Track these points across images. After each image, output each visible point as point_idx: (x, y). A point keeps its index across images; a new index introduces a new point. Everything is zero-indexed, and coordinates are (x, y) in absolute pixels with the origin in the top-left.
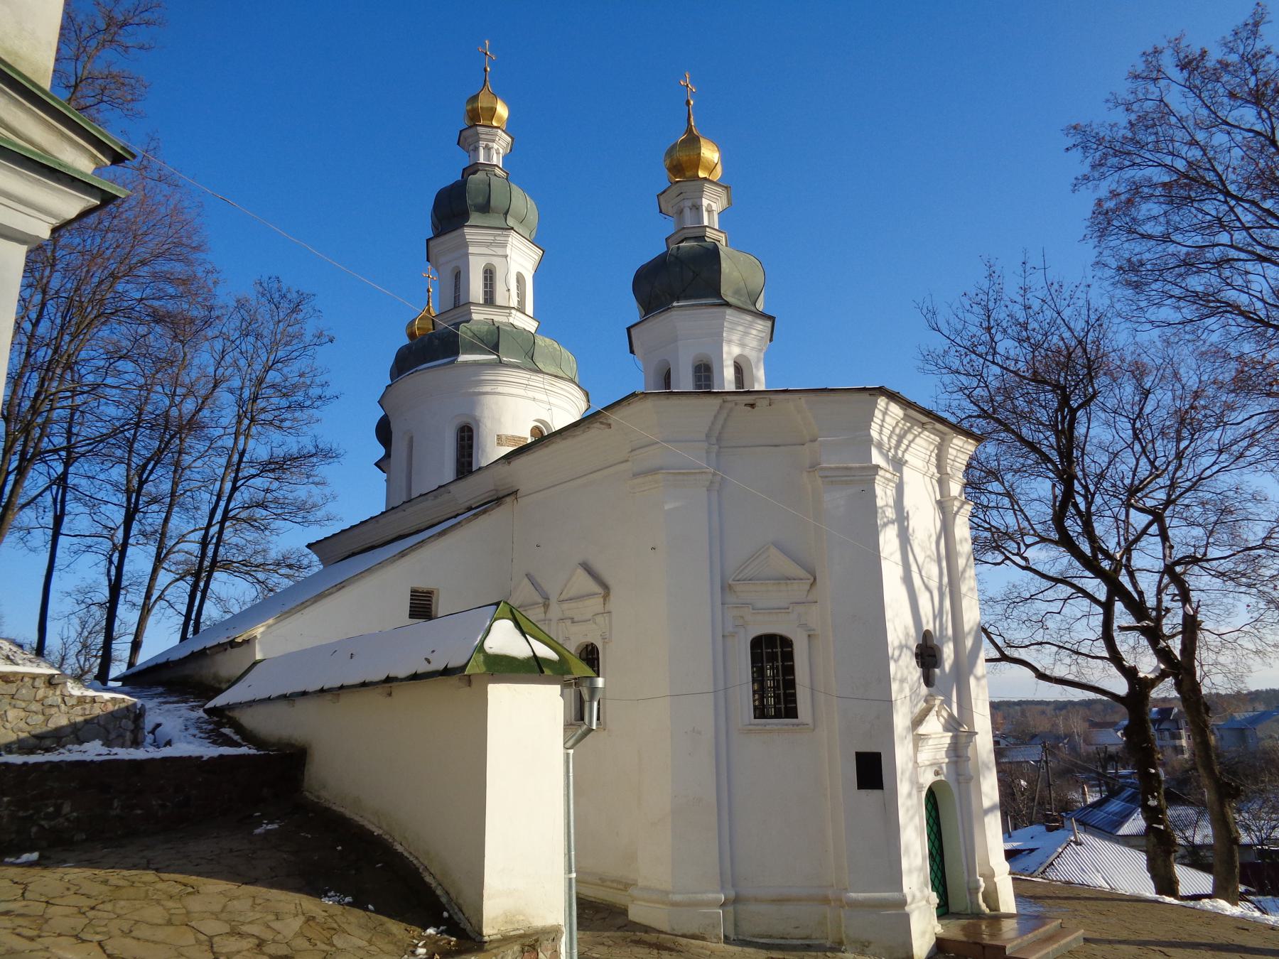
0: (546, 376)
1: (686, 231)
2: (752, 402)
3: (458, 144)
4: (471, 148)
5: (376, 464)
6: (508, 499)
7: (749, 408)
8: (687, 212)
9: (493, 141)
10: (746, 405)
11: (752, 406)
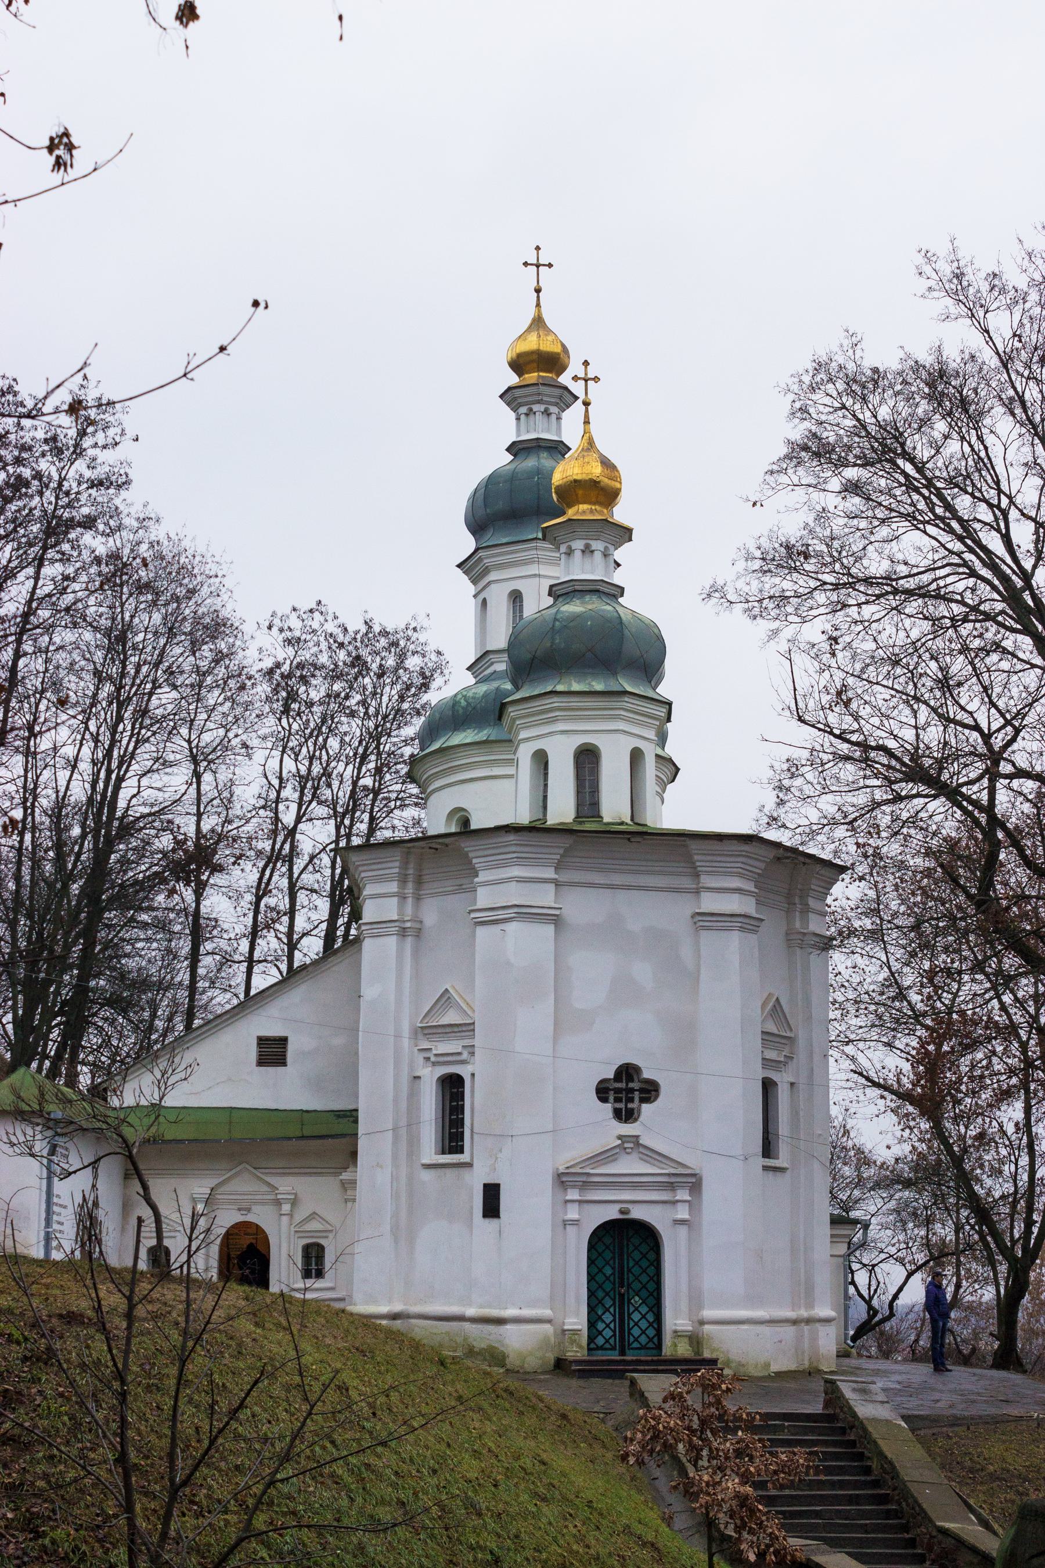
9: (539, 402)
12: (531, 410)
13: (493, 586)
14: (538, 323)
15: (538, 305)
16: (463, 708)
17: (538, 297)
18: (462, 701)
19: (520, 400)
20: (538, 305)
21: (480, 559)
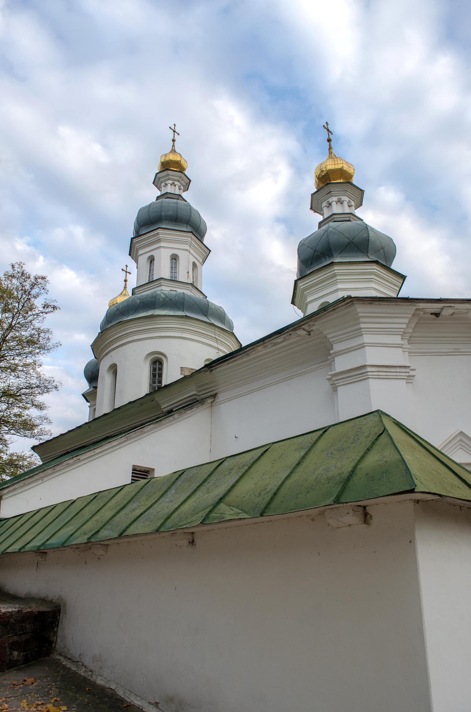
0: (217, 329)
1: (335, 216)
2: (437, 311)
3: (153, 183)
4: (163, 184)
5: (83, 395)
6: (209, 401)
7: (433, 316)
8: (334, 204)
9: (179, 181)
10: (432, 314)
11: (437, 315)
12: (173, 183)
13: (162, 249)
14: (173, 151)
15: (173, 146)
16: (163, 298)
17: (174, 143)
18: (162, 295)
19: (170, 177)
20: (173, 146)
21: (158, 234)
